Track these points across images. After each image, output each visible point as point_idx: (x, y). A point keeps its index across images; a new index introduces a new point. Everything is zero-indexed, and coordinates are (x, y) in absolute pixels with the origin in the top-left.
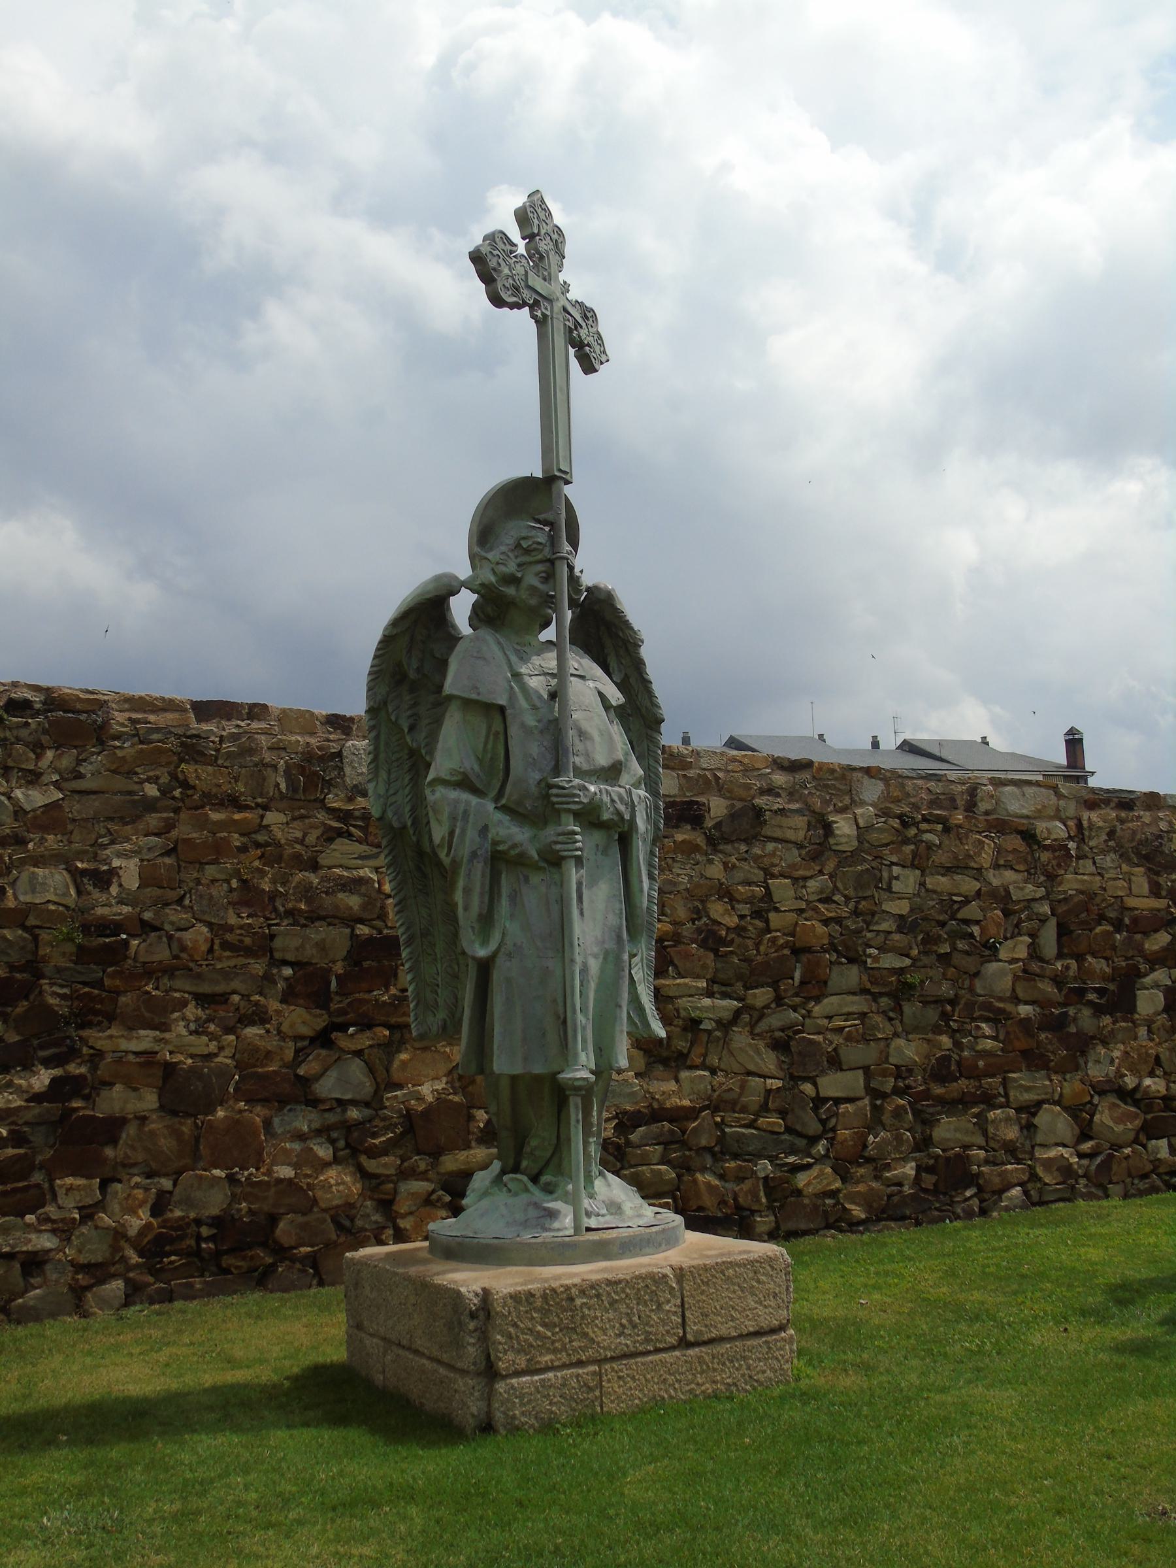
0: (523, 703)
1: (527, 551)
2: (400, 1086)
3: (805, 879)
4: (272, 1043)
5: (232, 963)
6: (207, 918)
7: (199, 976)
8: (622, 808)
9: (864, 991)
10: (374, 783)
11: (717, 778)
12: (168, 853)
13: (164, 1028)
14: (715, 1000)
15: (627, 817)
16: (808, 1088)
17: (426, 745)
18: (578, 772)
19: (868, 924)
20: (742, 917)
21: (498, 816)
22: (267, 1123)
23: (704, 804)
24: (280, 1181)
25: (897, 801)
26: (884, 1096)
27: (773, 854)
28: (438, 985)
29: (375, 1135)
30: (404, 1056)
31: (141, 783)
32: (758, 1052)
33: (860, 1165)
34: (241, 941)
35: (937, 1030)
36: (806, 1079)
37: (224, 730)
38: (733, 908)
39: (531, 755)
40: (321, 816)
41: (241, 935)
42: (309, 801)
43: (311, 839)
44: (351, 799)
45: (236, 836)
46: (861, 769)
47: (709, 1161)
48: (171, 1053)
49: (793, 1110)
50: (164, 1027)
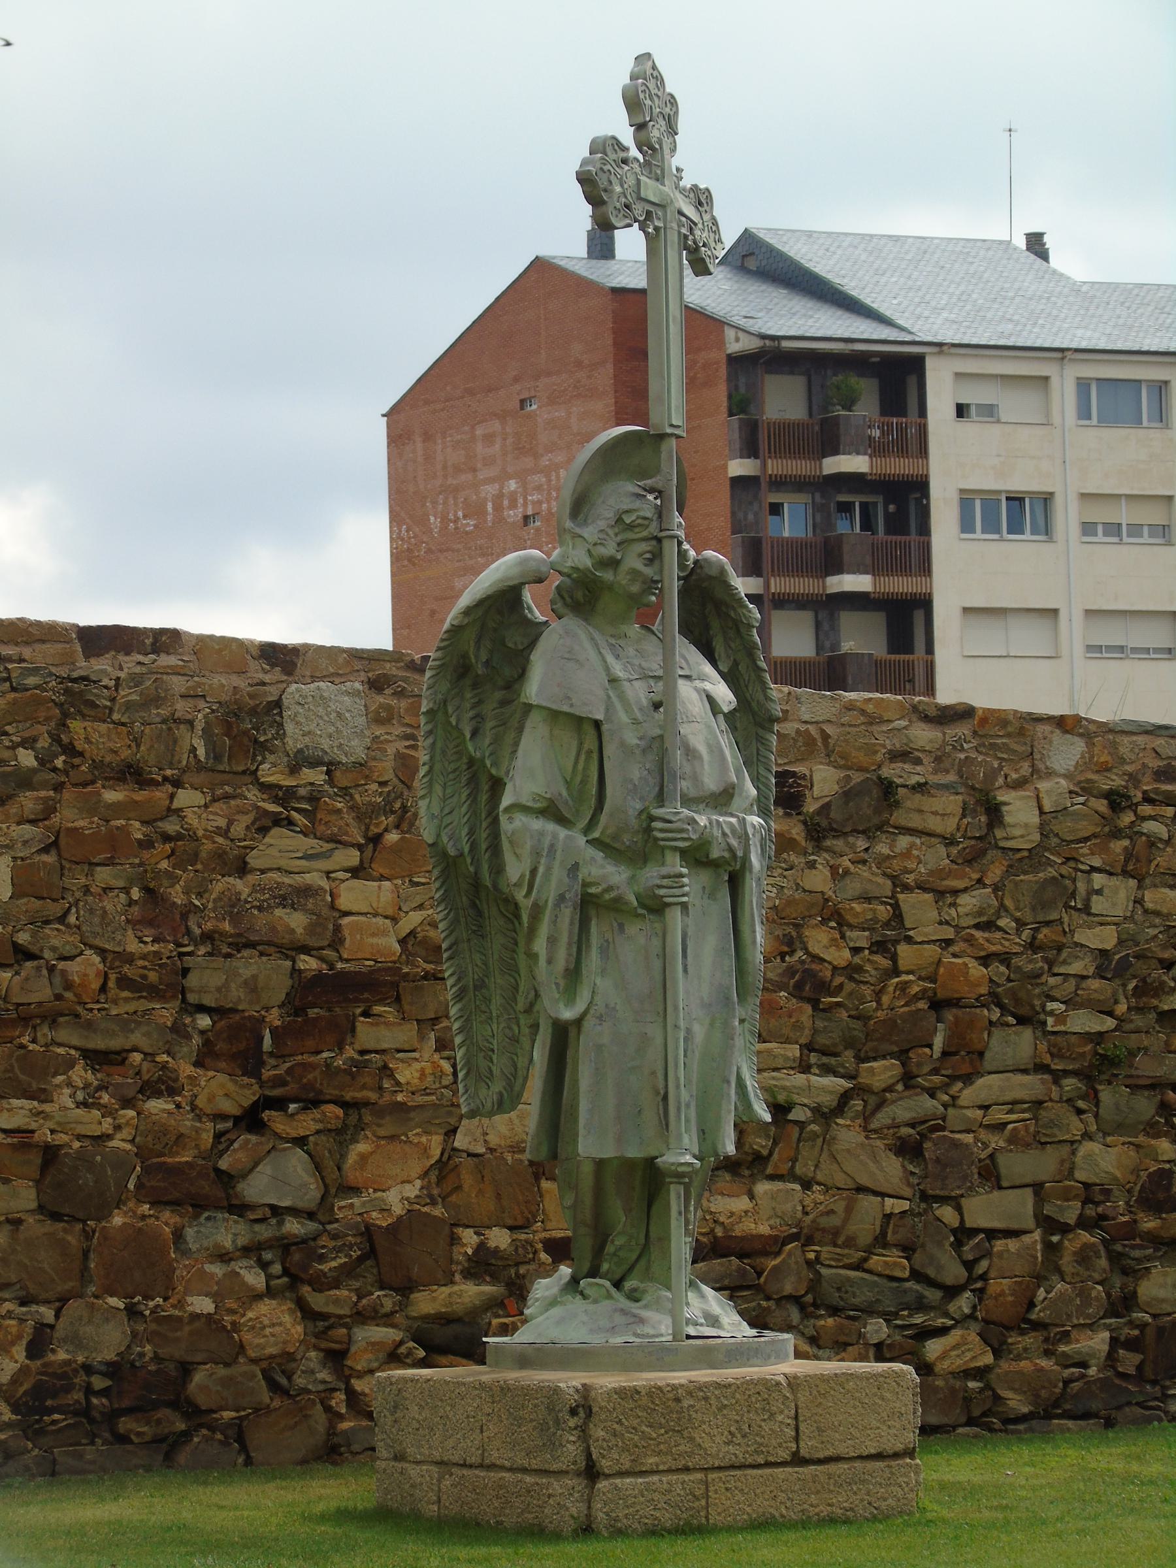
0: (624, 718)
1: (631, 527)
2: (355, 1190)
3: (956, 892)
4: (187, 1123)
5: (131, 1007)
6: (98, 942)
7: (89, 1025)
8: (734, 842)
9: (1041, 1068)
10: (427, 800)
11: (825, 737)
12: (46, 850)
13: (43, 1097)
14: (813, 1078)
15: (740, 854)
16: (947, 1214)
17: (491, 754)
18: (687, 801)
19: (1051, 963)
20: (856, 950)
21: (591, 852)
22: (178, 1235)
23: (804, 777)
24: (195, 1317)
25: (1105, 769)
26: (1065, 1229)
27: (907, 854)
28: (493, 1051)
29: (322, 1258)
30: (362, 1147)
31: (13, 747)
32: (874, 1158)
33: (1023, 1333)
34: (144, 977)
35: (1152, 1130)
36: (943, 1200)
37: (121, 669)
38: (843, 937)
39: (631, 780)
40: (253, 795)
41: (145, 968)
42: (235, 773)
43: (238, 830)
44: (294, 770)
45: (137, 824)
46: (1049, 719)
47: (795, 1315)
48: (52, 1132)
49: (923, 1246)
50: (43, 1096)
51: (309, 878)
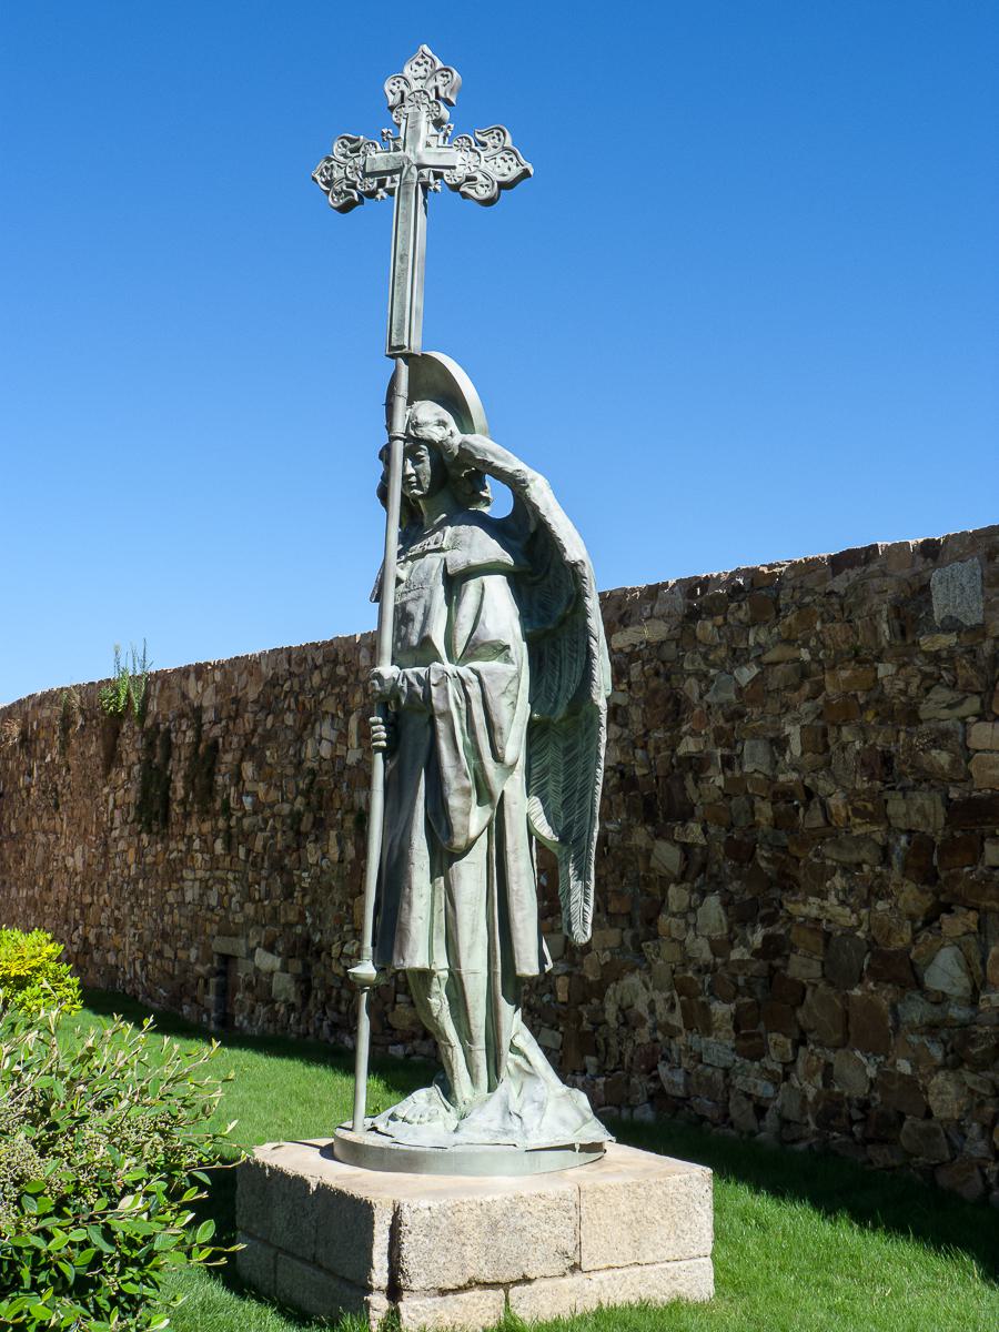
24: (902, 1075)
34: (865, 807)
43: (913, 690)
51: (949, 724)
